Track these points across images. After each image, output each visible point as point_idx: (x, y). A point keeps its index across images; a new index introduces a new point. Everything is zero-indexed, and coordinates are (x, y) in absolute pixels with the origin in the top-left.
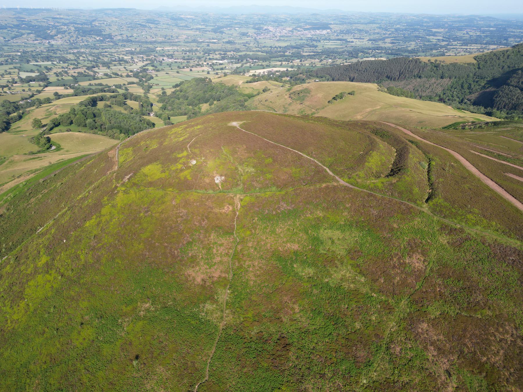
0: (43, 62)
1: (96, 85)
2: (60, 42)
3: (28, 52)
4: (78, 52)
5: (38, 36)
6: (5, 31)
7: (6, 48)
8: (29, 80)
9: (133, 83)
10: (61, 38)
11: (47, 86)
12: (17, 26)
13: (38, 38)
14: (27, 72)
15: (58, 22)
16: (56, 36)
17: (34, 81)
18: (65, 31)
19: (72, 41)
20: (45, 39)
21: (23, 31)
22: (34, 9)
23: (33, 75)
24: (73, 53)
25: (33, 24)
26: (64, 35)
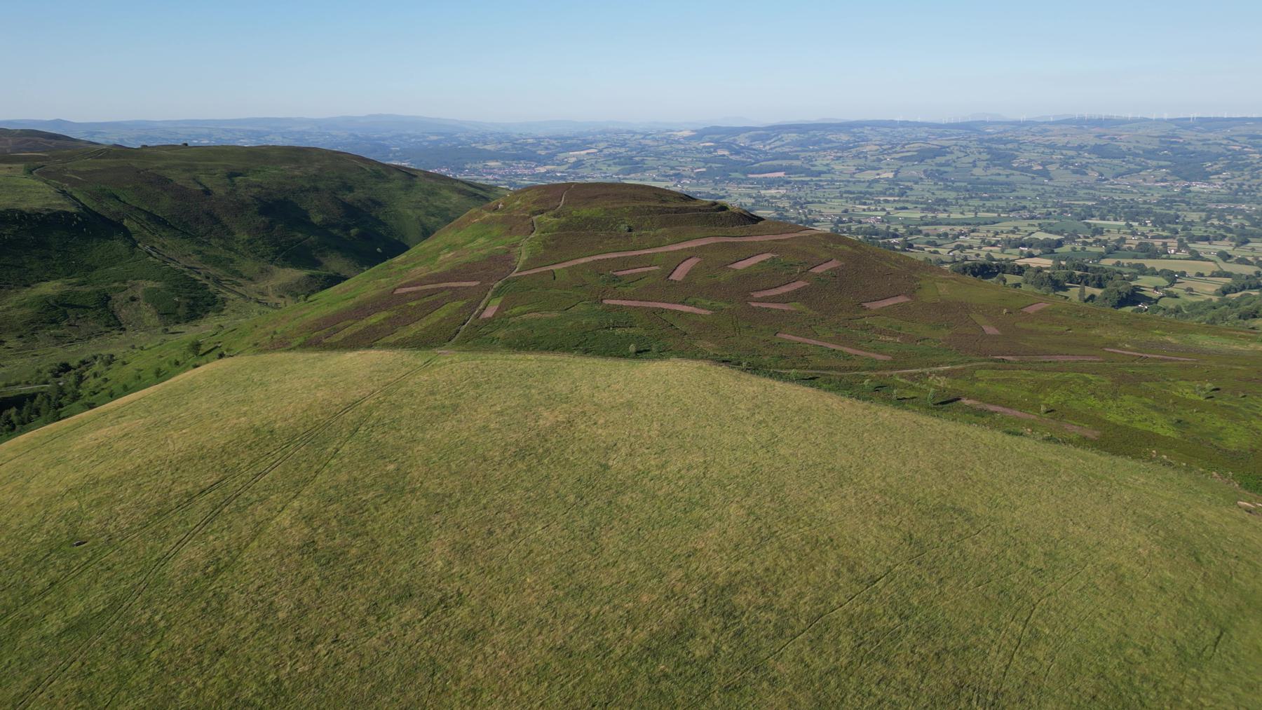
0: (1116, 220)
1: (1130, 265)
2: (1211, 188)
3: (1114, 201)
4: (1223, 210)
5: (1174, 173)
6: (1116, 161)
7: (1081, 193)
8: (1030, 244)
9: (1228, 275)
10: (1225, 180)
11: (1031, 256)
12: (1151, 154)
13: (1169, 178)
14: (1050, 232)
15: (1255, 146)
16: (1217, 173)
17: (1030, 246)
18: (1247, 165)
19: (1245, 187)
20: (1186, 179)
21: (1155, 163)
22: (1229, 119)
23: (1042, 236)
24: (1210, 212)
25: (1191, 148)
26: (1236, 173)
